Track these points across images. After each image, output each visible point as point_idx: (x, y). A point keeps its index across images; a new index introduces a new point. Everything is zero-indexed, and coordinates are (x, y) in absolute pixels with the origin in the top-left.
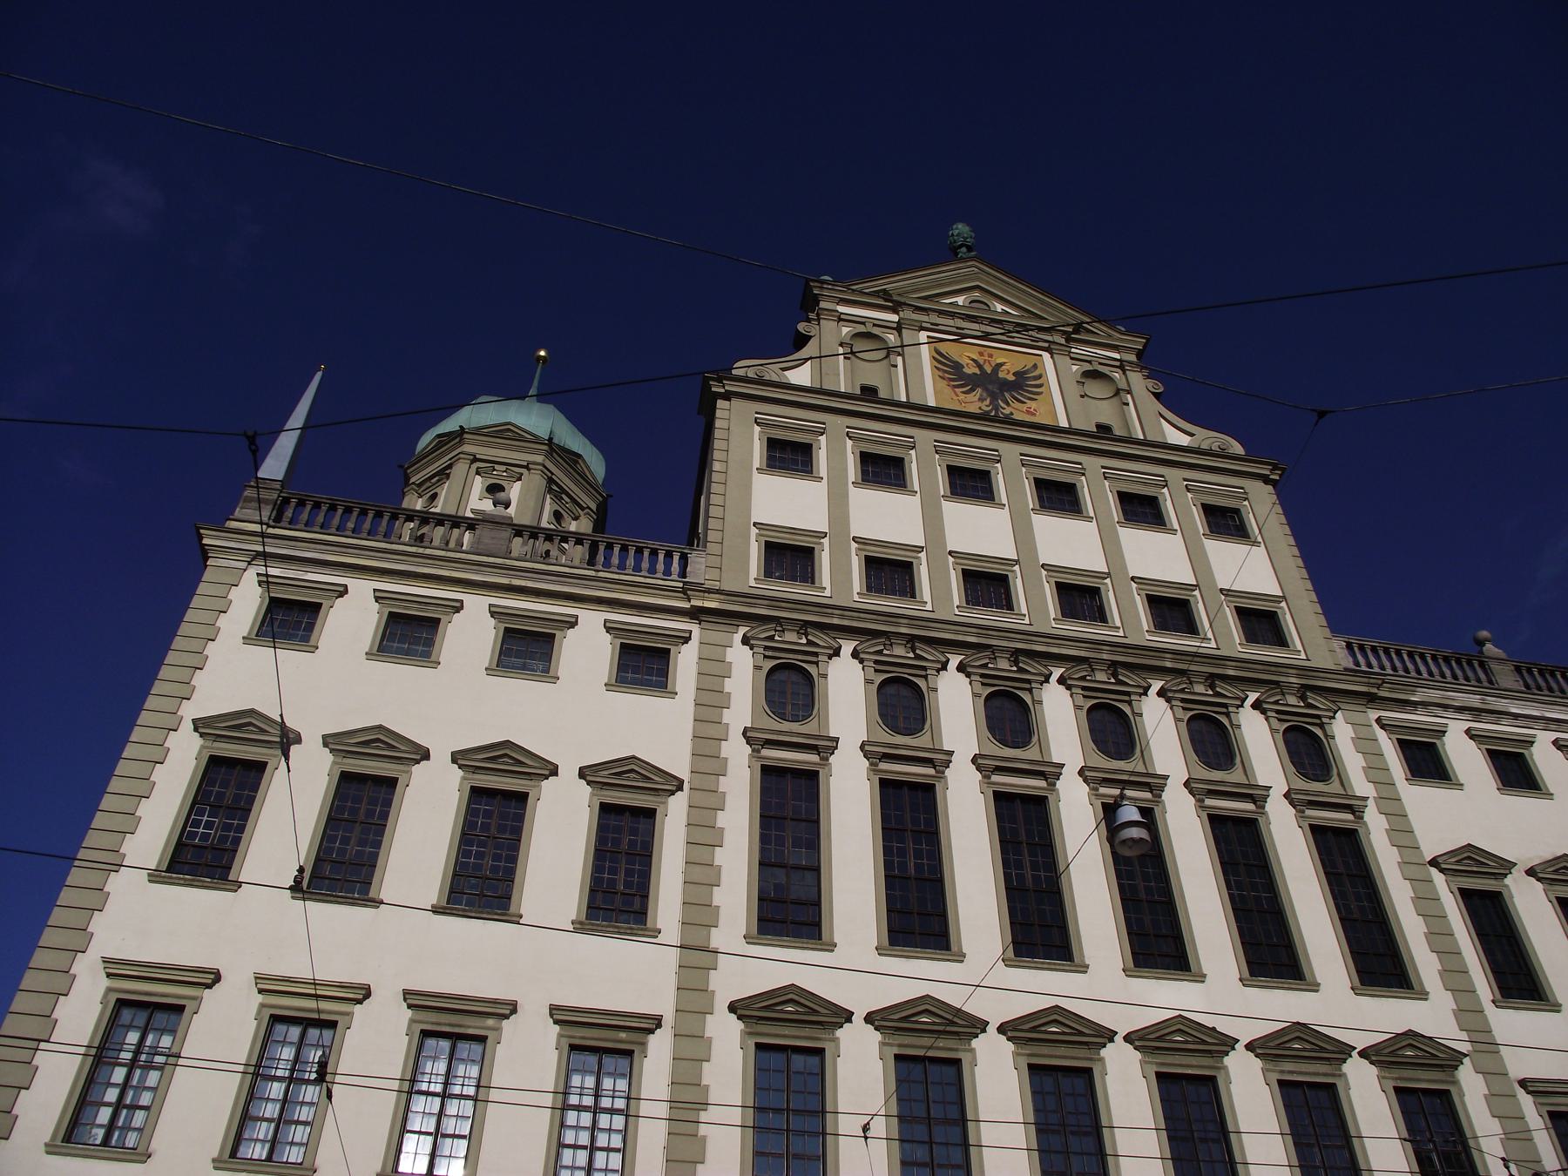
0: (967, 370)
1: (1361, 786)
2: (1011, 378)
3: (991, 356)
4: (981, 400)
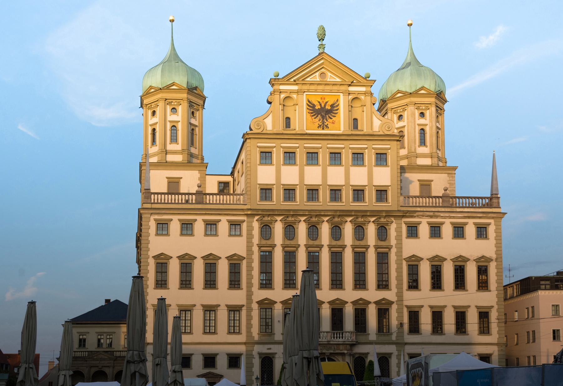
0: (317, 108)
1: (393, 241)
2: (329, 108)
3: (324, 99)
4: (319, 120)
